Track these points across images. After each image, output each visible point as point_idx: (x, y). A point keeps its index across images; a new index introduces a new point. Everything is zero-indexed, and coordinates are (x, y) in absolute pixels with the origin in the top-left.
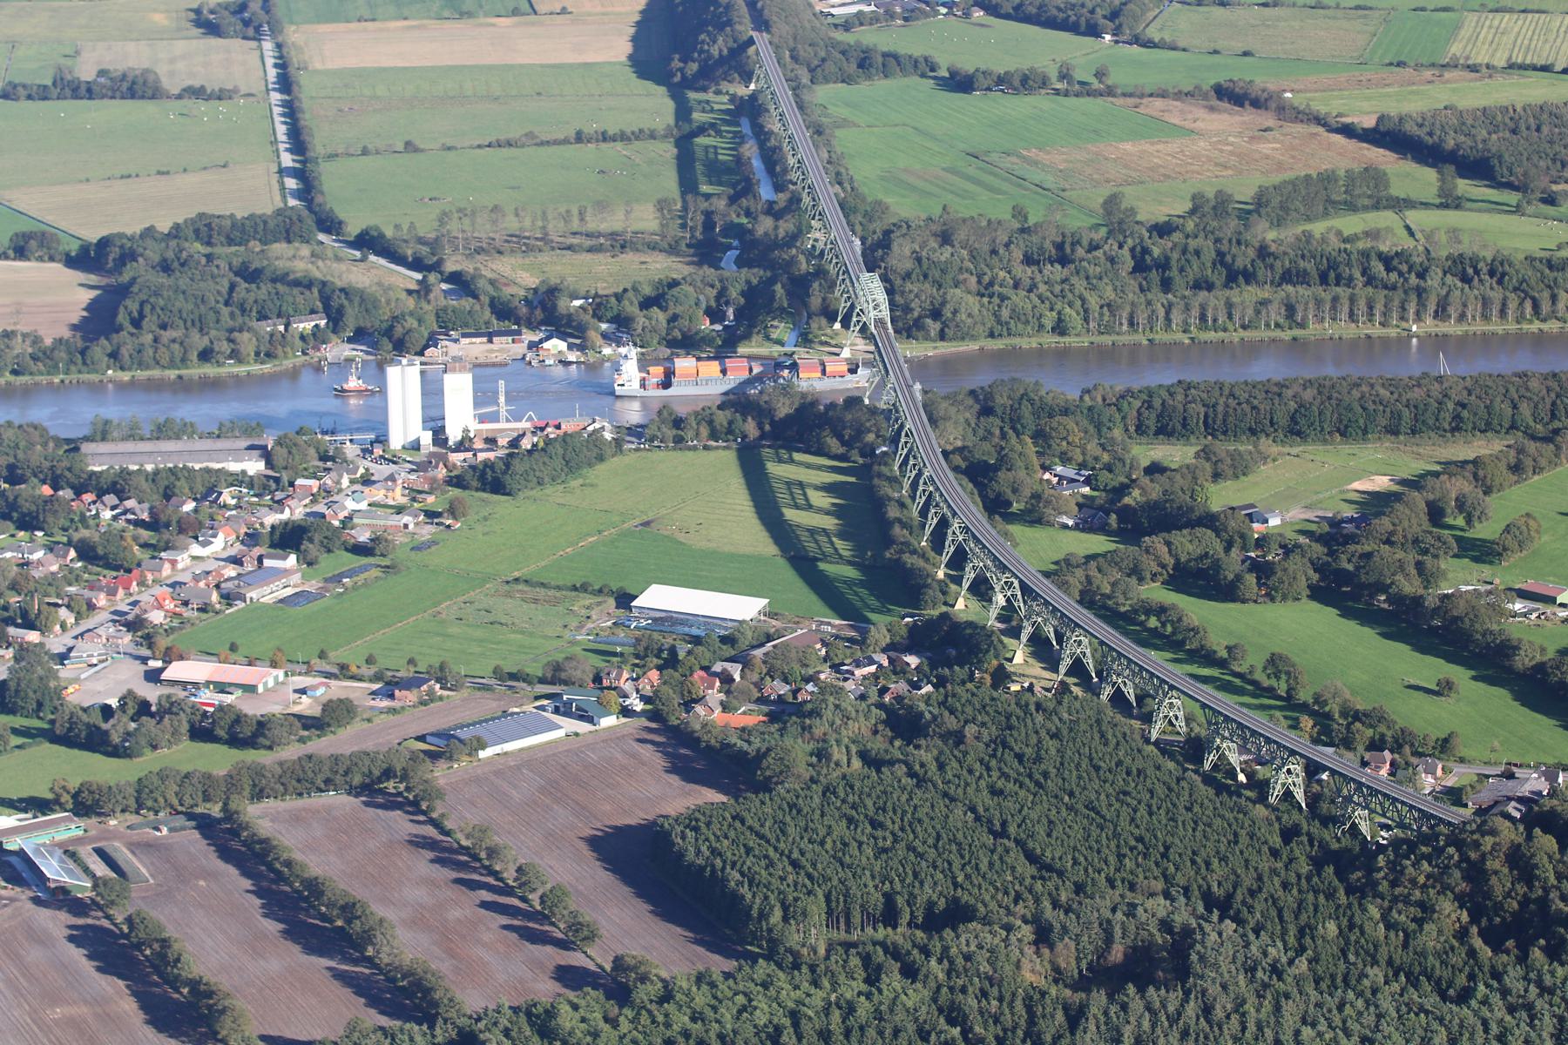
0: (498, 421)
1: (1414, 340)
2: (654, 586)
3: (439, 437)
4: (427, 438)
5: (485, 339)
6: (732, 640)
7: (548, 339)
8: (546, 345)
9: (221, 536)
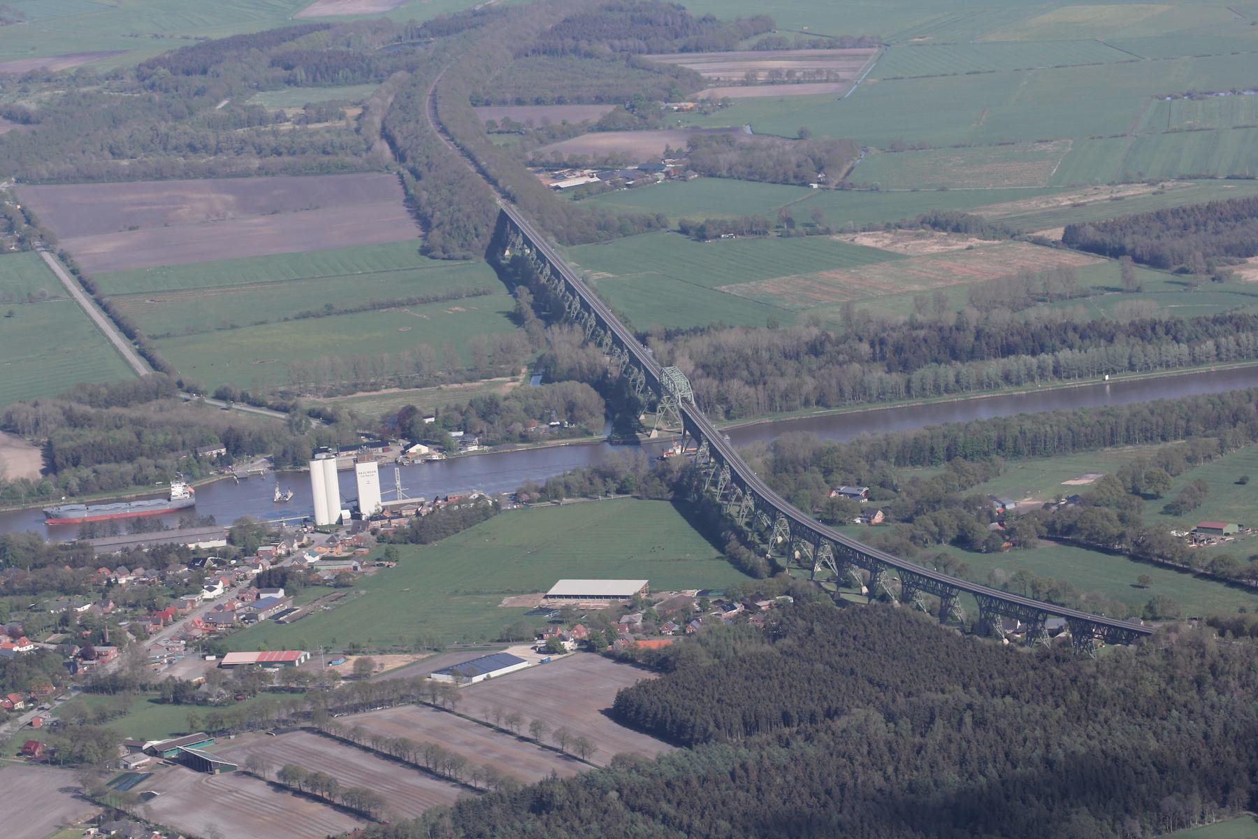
0: (397, 499)
1: (1108, 387)
2: (561, 581)
3: (356, 514)
4: (347, 514)
6: (632, 604)
7: (412, 445)
8: (412, 450)
9: (221, 583)
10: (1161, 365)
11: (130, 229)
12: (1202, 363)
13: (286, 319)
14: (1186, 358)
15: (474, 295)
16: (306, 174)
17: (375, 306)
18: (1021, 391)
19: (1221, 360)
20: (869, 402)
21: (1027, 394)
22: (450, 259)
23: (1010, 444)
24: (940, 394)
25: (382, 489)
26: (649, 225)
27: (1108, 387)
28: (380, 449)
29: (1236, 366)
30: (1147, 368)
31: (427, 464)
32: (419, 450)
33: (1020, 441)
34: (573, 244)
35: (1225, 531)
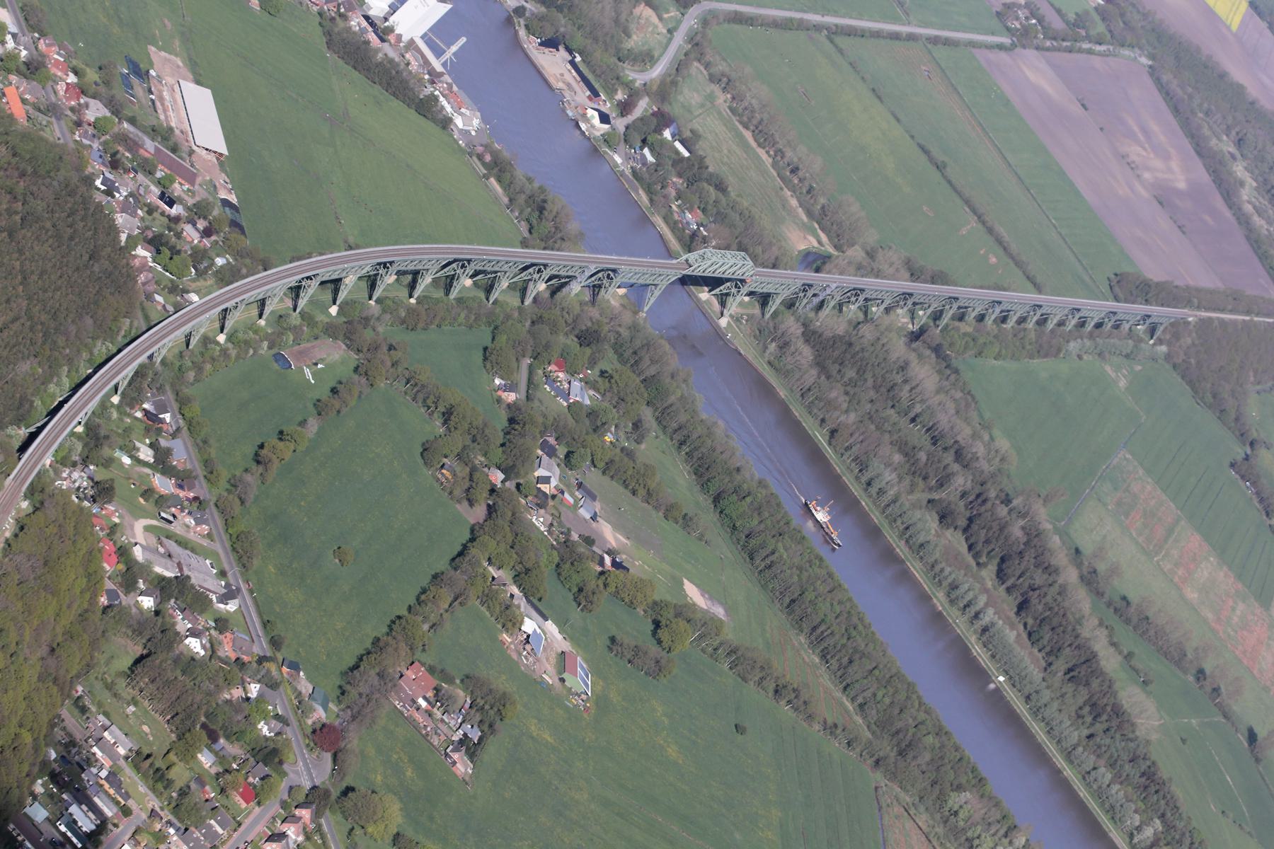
1: (992, 686)
2: (208, 92)
5: (579, 79)
10: (1047, 724)
11: (1083, 105)
12: (1071, 762)
13: (912, 137)
14: (1067, 744)
15: (1028, 278)
16: (1251, 245)
17: (967, 202)
18: (942, 605)
19: (1084, 778)
20: (857, 478)
21: (940, 613)
22: (1111, 288)
23: (753, 542)
24: (901, 536)
25: (431, 30)
26: (1242, 435)
27: (992, 686)
28: (588, 93)
29: (1083, 793)
30: (1035, 712)
31: (574, 123)
32: (593, 116)
33: (763, 553)
34: (1183, 378)
35: (565, 676)
